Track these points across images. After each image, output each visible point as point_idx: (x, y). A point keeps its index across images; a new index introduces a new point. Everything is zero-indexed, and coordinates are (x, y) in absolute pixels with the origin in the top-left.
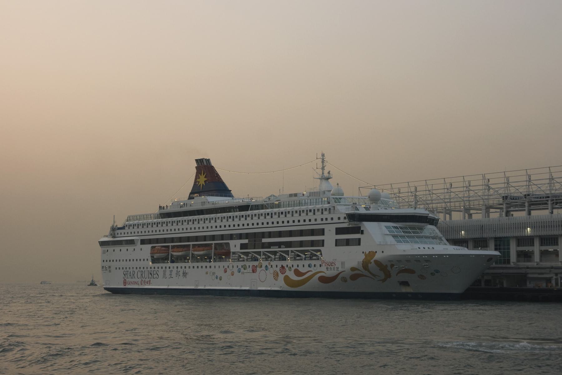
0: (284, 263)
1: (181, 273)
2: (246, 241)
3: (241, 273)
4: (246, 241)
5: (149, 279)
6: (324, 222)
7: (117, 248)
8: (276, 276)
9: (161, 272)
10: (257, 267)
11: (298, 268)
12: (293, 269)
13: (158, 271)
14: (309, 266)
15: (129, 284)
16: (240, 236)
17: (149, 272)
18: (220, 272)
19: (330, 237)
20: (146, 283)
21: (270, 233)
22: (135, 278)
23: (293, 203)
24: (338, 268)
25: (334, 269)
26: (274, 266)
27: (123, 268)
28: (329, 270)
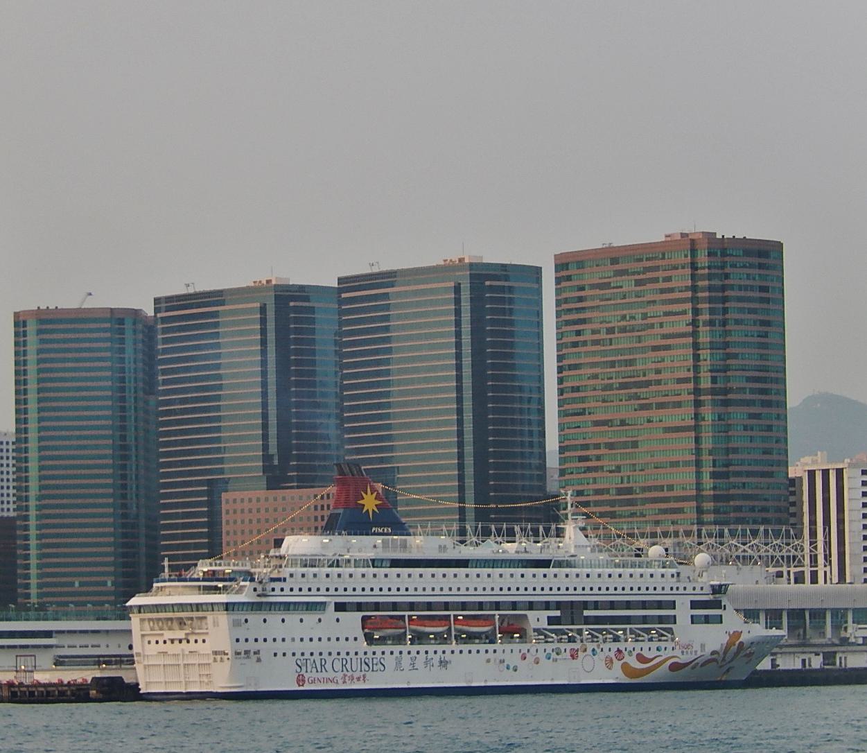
0: (621, 645)
1: (436, 663)
2: (558, 613)
3: (551, 659)
4: (558, 613)
5: (363, 673)
6: (675, 591)
7: (274, 618)
8: (609, 663)
9: (389, 661)
10: (577, 650)
11: (641, 652)
12: (635, 654)
13: (384, 659)
14: (658, 649)
15: (313, 682)
16: (547, 606)
17: (363, 660)
18: (514, 660)
19: (683, 612)
20: (355, 680)
21: (596, 602)
22: (326, 671)
23: (597, 562)
24: (696, 652)
25: (691, 653)
26: (606, 650)
27: (294, 654)
28: (685, 653)
